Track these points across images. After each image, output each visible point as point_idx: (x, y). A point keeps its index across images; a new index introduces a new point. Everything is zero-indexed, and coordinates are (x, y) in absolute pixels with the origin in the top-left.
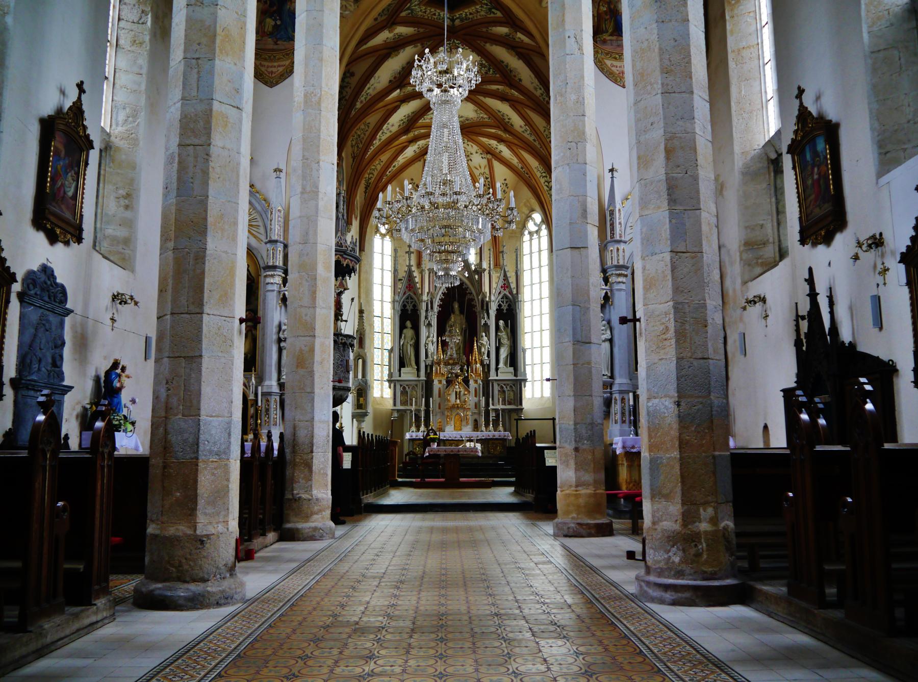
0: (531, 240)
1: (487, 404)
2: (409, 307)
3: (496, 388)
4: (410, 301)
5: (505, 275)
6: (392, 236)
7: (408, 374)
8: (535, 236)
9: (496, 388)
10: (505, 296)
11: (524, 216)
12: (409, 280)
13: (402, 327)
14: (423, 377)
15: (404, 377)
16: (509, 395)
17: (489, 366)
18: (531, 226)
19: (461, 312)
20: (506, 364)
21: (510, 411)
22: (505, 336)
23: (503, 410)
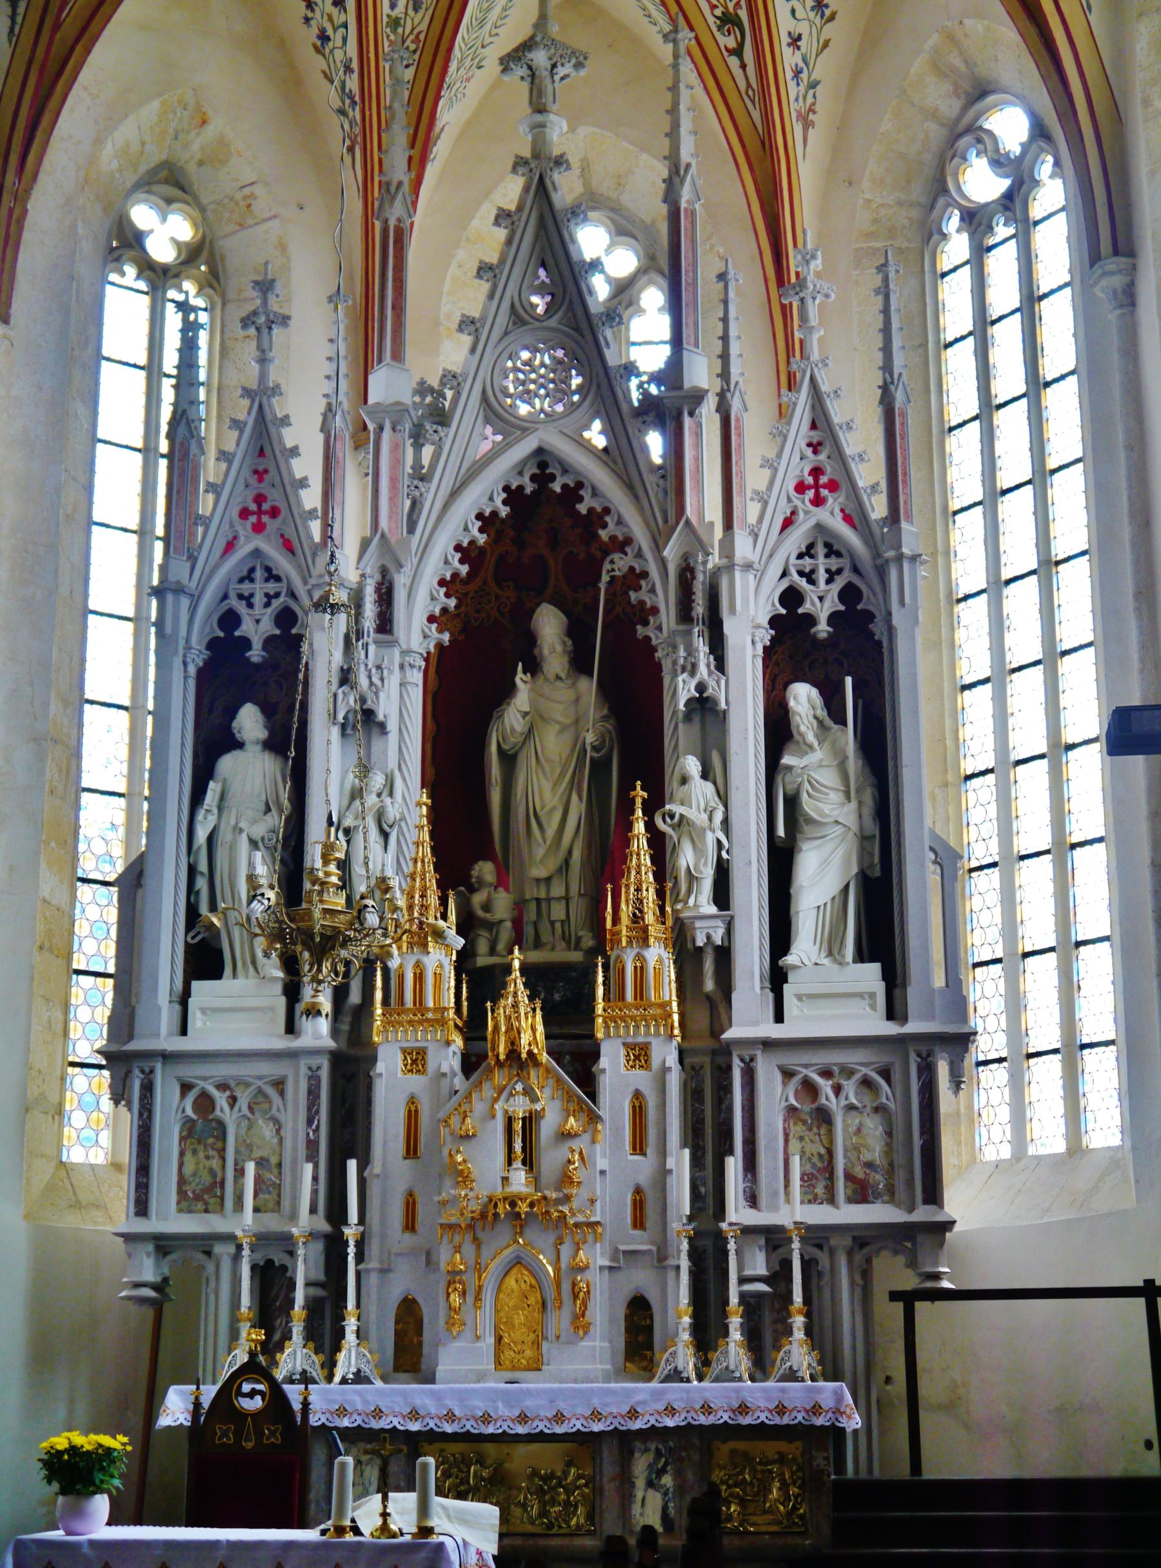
0: (980, 252)
1: (709, 1198)
2: (257, 627)
3: (774, 1096)
4: (259, 588)
5: (820, 420)
6: (213, 282)
7: (238, 1014)
8: (1002, 231)
11: (936, 133)
12: (260, 474)
13: (213, 743)
14: (318, 1032)
15: (207, 1033)
16: (860, 1136)
17: (724, 955)
18: (981, 183)
20: (832, 948)
21: (864, 1239)
22: (828, 777)
23: (817, 1236)
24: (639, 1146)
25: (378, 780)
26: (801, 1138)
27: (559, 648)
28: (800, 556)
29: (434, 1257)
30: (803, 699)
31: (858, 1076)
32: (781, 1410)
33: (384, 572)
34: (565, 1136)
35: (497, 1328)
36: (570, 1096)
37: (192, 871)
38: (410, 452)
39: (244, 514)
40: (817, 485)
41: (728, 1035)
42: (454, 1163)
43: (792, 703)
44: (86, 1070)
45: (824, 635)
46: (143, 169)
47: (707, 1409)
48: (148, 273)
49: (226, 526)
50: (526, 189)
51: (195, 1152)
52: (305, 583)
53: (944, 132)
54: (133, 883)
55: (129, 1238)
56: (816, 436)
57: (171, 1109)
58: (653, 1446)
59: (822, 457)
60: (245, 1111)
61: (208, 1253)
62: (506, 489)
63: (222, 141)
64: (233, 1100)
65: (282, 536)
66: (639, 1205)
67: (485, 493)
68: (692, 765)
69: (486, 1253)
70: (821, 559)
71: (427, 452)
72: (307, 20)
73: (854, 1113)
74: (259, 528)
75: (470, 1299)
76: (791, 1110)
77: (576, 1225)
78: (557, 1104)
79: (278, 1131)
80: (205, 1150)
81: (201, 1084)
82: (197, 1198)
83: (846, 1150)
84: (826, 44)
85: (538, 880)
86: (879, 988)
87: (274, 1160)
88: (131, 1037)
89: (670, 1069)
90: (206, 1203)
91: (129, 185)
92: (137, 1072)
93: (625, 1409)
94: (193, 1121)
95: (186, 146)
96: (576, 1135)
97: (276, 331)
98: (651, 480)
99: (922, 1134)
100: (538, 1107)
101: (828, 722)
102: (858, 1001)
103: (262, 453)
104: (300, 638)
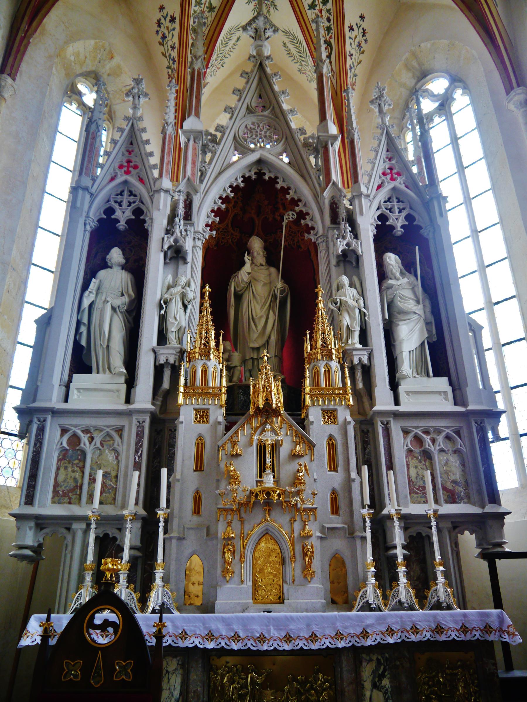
3: (400, 444)
7: (97, 392)
9: (400, 444)
10: (396, 196)
11: (404, 92)
13: (95, 264)
16: (449, 466)
17: (367, 371)
19: (271, 260)
20: (421, 370)
22: (408, 293)
24: (333, 467)
25: (183, 280)
26: (416, 467)
27: (261, 253)
28: (385, 202)
29: (212, 530)
30: (393, 259)
31: (444, 434)
32: (464, 629)
33: (188, 195)
34: (295, 456)
35: (254, 576)
36: (297, 434)
37: (79, 323)
38: (200, 156)
39: (121, 167)
40: (390, 173)
41: (375, 408)
42: (228, 471)
43: (388, 260)
44: (11, 437)
45: (399, 233)
46: (84, 69)
47: (415, 630)
48: (82, 106)
49: (111, 170)
50: (255, 66)
51: (66, 468)
52: (149, 193)
53: (408, 92)
54: (45, 323)
55: (18, 517)
56: (390, 155)
57: (54, 441)
58: (374, 658)
59: (393, 162)
60: (98, 445)
61: (69, 529)
62: (243, 177)
63: (119, 67)
64: (92, 439)
65: (139, 177)
66: (334, 500)
67: (232, 176)
68: (345, 280)
69: (247, 527)
70: (395, 203)
71: (208, 156)
72: (157, 32)
73: (443, 454)
74: (128, 173)
75: (237, 556)
76: (410, 451)
77: (305, 510)
78: (289, 438)
79: (117, 457)
80: (72, 467)
81: (74, 429)
82: (65, 495)
83: (441, 474)
84: (360, 62)
85: (253, 349)
86: (449, 390)
87: (113, 474)
88: (34, 401)
89: (349, 423)
90: (70, 498)
91: (78, 73)
92: (35, 420)
93: (359, 630)
94: (67, 450)
95: (104, 66)
96: (302, 456)
97: (142, 100)
98: (312, 173)
99: (483, 465)
100: (280, 438)
101: (404, 271)
102: (437, 395)
103: (132, 137)
104: (144, 221)
